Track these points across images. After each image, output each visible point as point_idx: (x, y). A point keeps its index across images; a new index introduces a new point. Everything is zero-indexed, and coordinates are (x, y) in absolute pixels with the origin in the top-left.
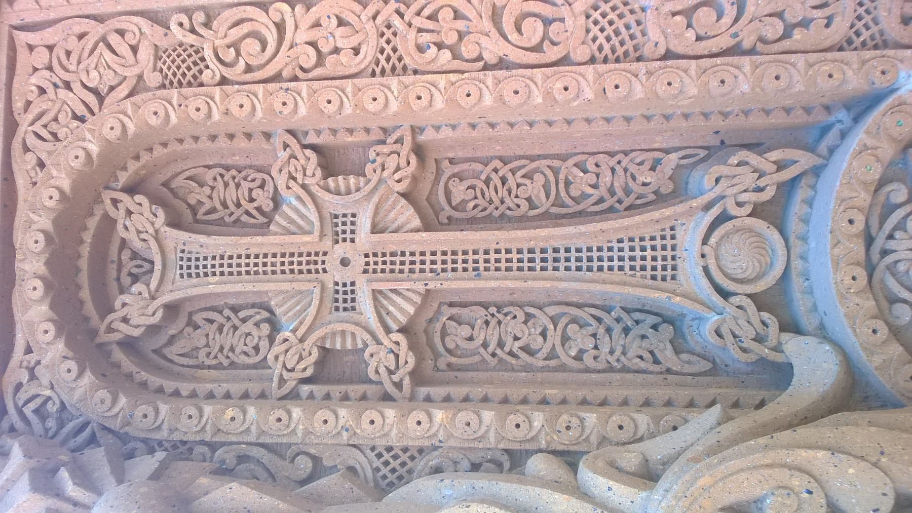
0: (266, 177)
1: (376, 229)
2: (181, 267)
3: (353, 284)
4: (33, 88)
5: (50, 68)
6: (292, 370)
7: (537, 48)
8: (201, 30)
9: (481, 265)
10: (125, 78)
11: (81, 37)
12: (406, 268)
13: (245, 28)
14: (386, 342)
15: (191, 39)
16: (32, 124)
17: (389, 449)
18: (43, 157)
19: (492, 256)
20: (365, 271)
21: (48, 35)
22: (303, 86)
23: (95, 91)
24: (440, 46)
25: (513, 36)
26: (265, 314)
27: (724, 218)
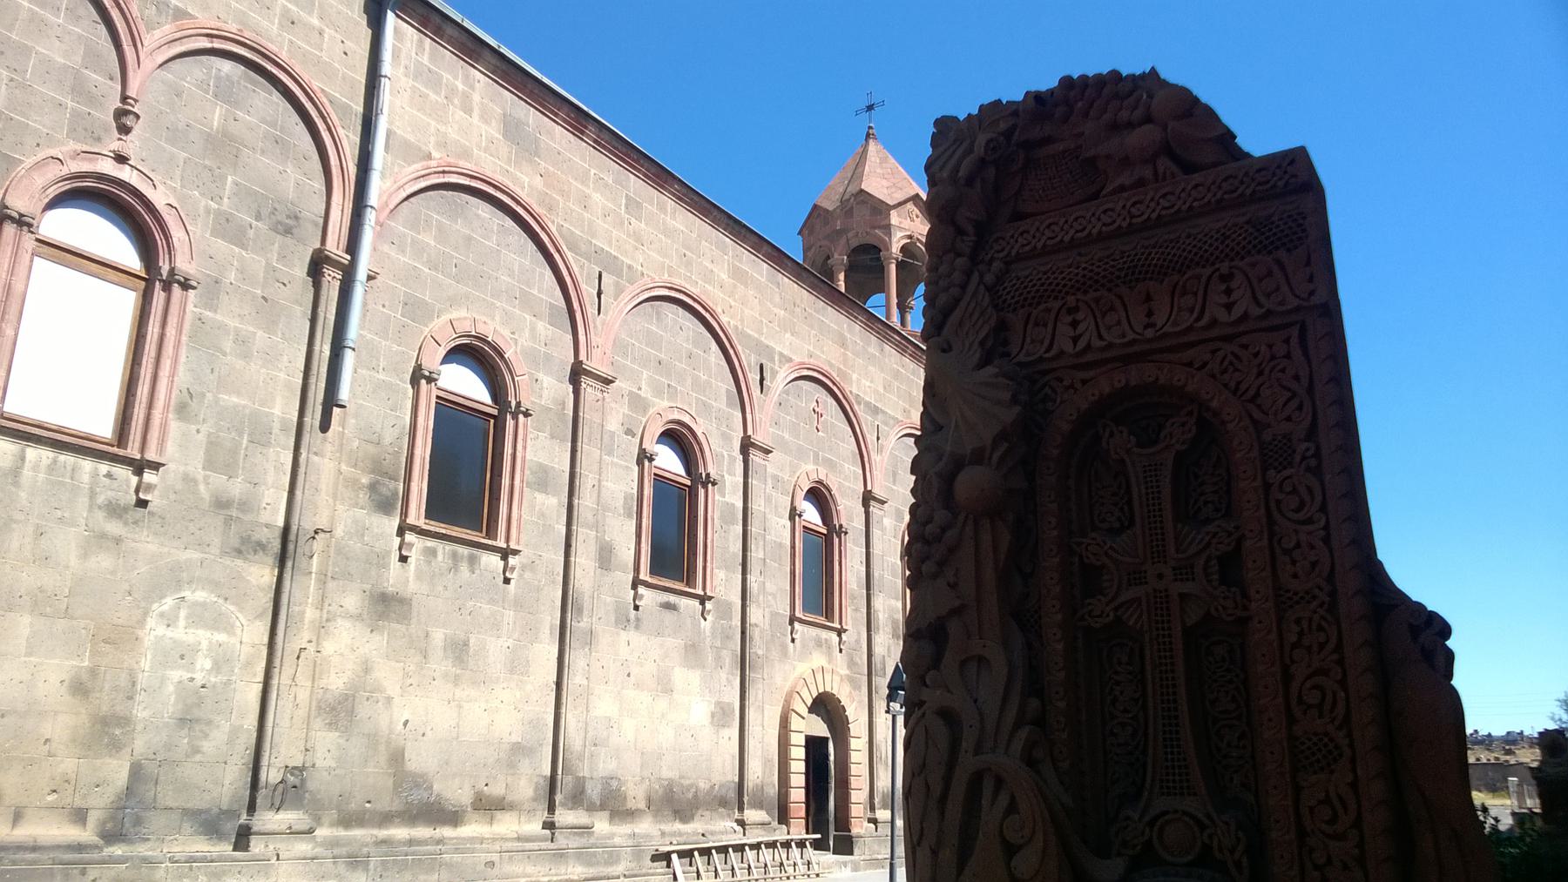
0: (1223, 512)
1: (1183, 596)
2: (1150, 465)
3: (1146, 583)
4: (1257, 349)
5: (1273, 358)
6: (1087, 550)
7: (1300, 701)
8: (1303, 466)
9: (1164, 668)
10: (1268, 415)
11: (1297, 378)
12: (1159, 618)
13: (1307, 498)
14: (1108, 609)
15: (1298, 458)
16: (1232, 353)
17: (1040, 617)
18: (1209, 366)
19: (1170, 675)
20: (1155, 590)
21: (1297, 353)
22: (1265, 542)
23: (1257, 395)
24: (1301, 634)
25: (1308, 684)
26: (1126, 524)
27: (1203, 827)
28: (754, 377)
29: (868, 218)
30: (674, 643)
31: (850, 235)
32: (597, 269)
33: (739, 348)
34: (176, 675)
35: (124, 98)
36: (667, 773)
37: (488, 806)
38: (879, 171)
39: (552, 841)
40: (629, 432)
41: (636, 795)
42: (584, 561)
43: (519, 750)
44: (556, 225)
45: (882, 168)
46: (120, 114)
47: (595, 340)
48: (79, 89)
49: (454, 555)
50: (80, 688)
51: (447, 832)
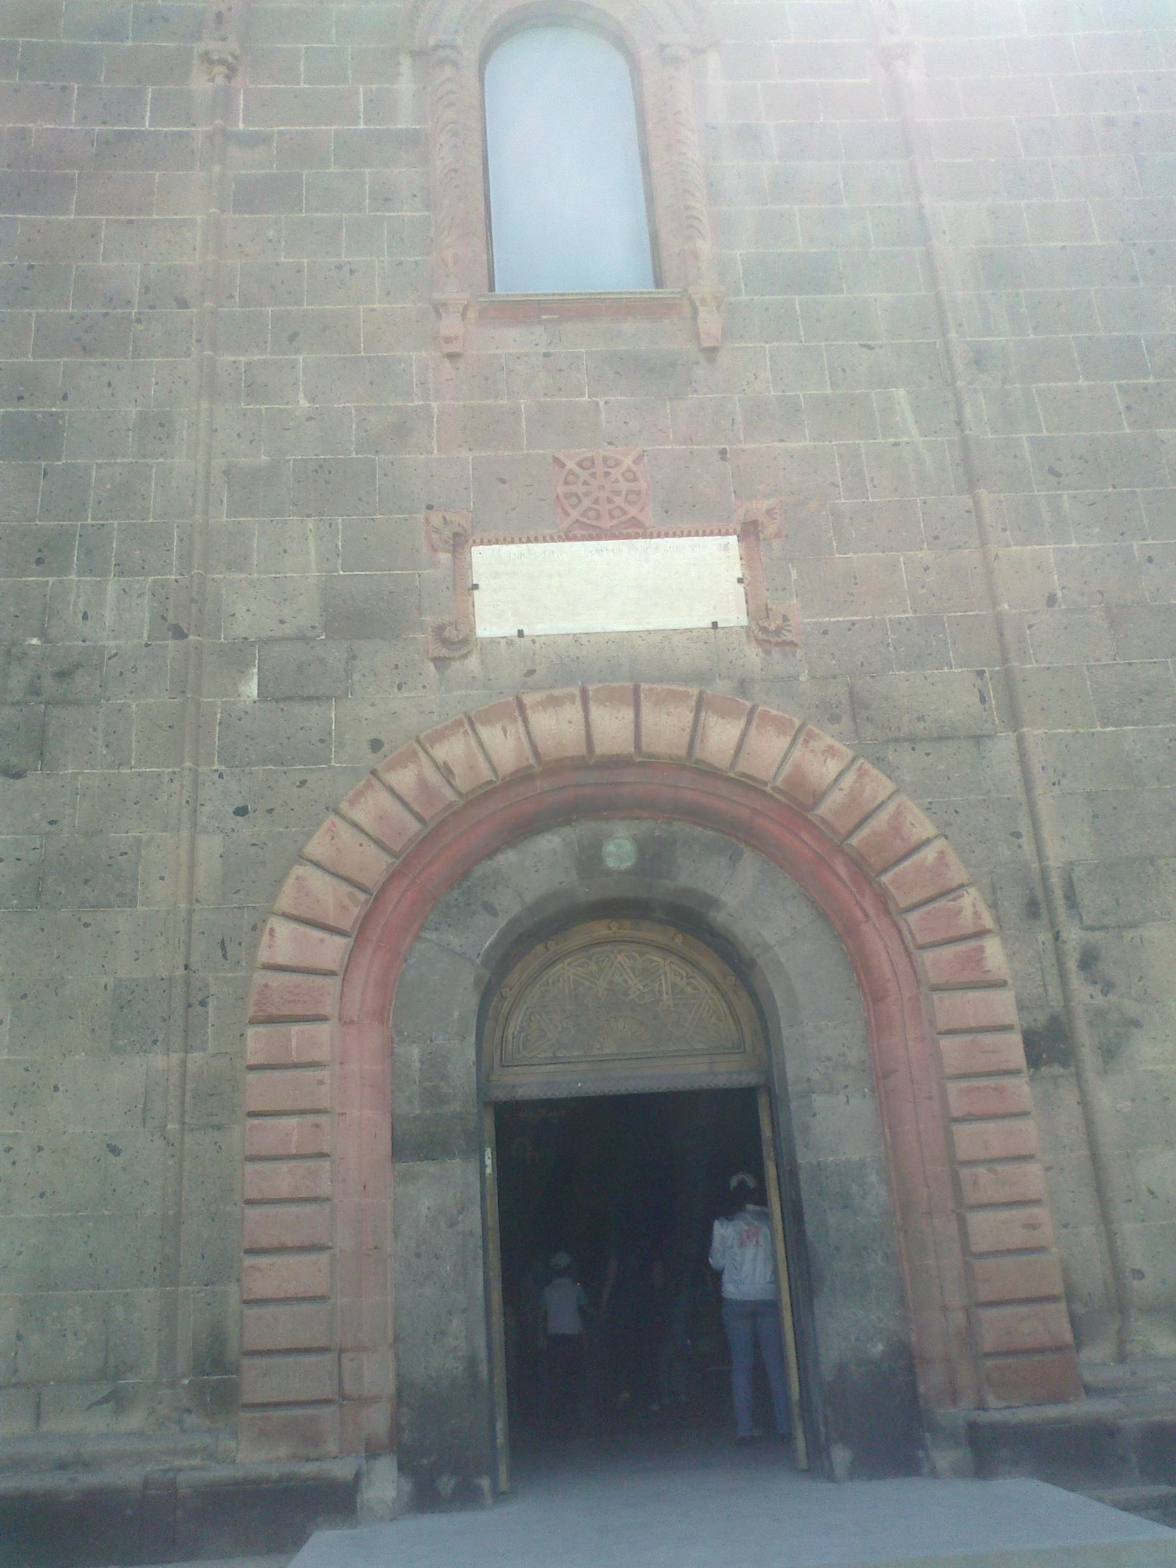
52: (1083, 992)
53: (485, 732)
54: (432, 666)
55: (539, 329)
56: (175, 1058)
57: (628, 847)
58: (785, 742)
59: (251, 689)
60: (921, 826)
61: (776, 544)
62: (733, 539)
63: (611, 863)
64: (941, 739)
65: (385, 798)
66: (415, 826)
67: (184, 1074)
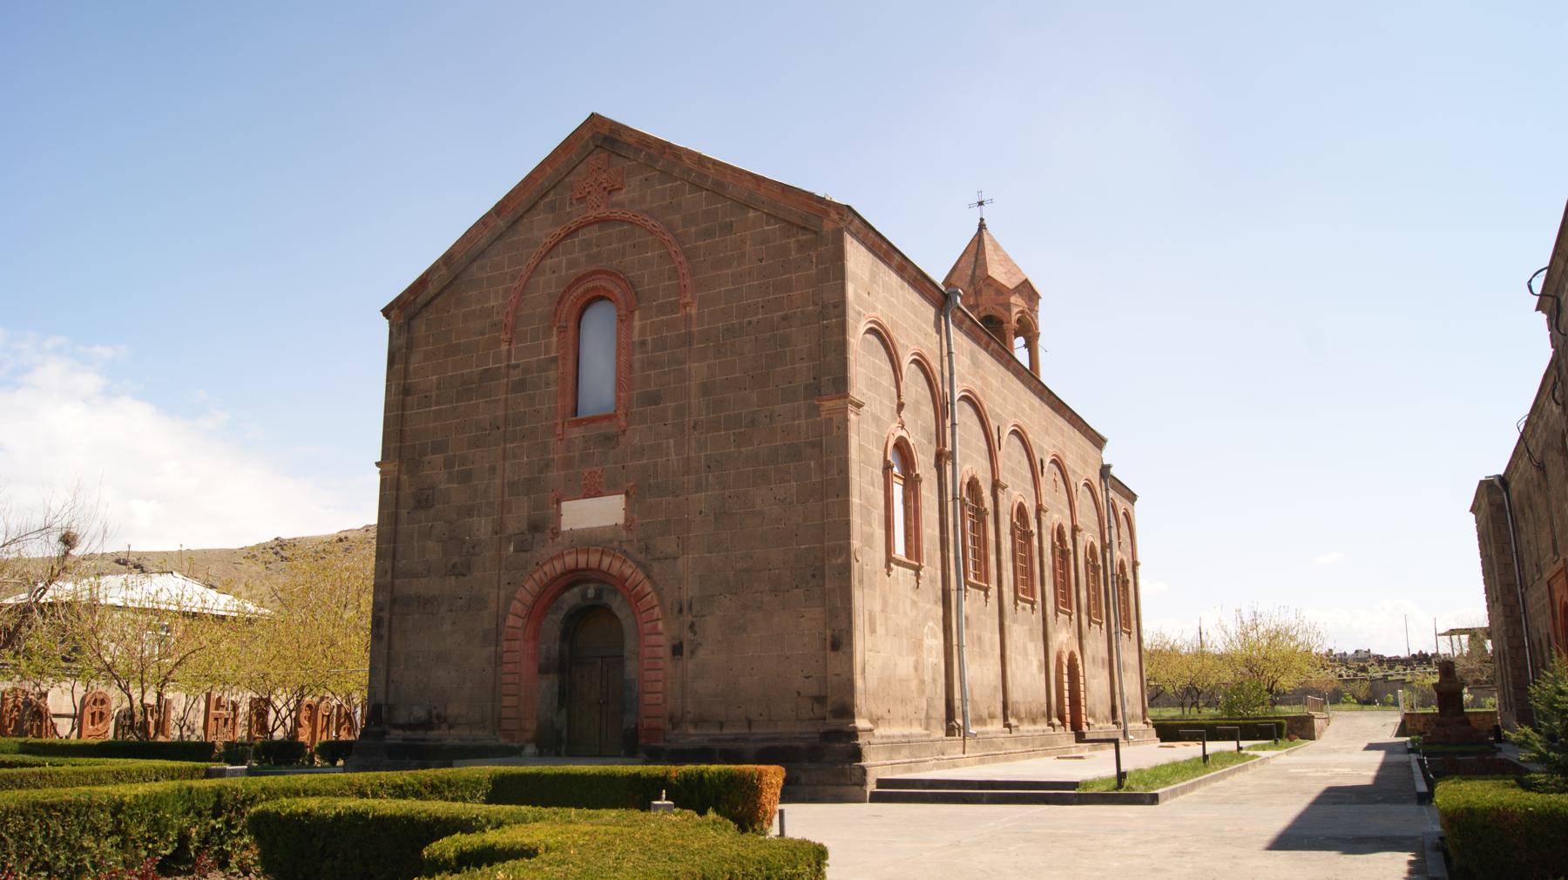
28: (1039, 467)
29: (993, 297)
30: (1026, 628)
31: (980, 309)
32: (997, 424)
33: (1034, 451)
34: (930, 659)
35: (899, 396)
36: (1030, 699)
37: (992, 716)
38: (996, 258)
39: (1011, 733)
40: (1008, 513)
41: (1022, 710)
42: (1005, 589)
43: (995, 687)
44: (987, 406)
45: (997, 255)
46: (901, 406)
47: (1000, 464)
48: (891, 400)
49: (975, 593)
50: (916, 669)
51: (984, 729)
52: (690, 635)
53: (555, 562)
54: (550, 541)
55: (582, 427)
56: (493, 649)
57: (593, 590)
58: (620, 564)
59: (512, 549)
60: (648, 588)
61: (634, 496)
62: (623, 496)
63: (589, 596)
64: (666, 558)
65: (531, 582)
66: (538, 589)
67: (496, 654)
